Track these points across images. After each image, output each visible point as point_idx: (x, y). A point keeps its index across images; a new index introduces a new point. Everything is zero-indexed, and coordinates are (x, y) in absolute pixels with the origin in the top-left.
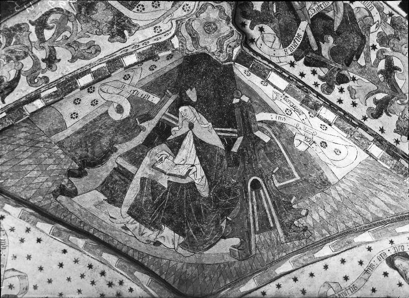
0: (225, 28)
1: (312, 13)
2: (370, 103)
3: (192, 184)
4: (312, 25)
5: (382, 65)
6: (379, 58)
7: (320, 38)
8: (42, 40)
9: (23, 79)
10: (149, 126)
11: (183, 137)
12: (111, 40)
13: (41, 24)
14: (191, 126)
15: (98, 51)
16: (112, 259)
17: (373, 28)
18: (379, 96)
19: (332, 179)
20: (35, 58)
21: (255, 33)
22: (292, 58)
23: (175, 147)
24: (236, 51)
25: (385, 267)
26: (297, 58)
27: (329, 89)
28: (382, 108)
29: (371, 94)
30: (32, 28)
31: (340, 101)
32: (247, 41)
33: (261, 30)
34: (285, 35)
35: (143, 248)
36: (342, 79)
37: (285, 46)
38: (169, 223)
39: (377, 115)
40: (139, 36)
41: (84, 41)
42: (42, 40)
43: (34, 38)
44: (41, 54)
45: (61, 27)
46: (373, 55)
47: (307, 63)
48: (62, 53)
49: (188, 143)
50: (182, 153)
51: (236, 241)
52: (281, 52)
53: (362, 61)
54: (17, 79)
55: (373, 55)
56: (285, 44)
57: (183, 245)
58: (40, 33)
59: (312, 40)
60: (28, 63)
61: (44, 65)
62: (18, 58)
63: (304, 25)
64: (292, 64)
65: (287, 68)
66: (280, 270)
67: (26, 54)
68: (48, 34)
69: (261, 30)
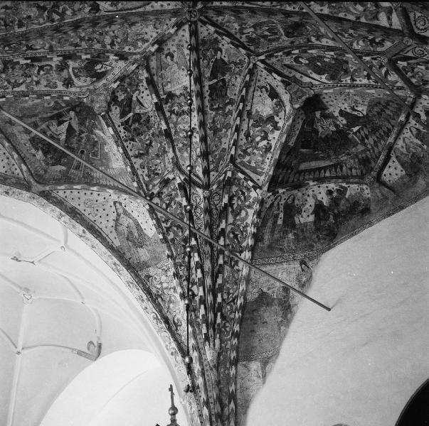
2: (137, 152)
4: (133, 116)
5: (148, 142)
6: (148, 140)
7: (134, 122)
10: (56, 112)
11: (66, 121)
12: (63, 85)
14: (71, 119)
15: (56, 87)
16: (16, 156)
18: (141, 152)
19: (110, 166)
20: (32, 79)
21: (113, 108)
23: (60, 123)
24: (103, 114)
25: (112, 204)
26: (122, 125)
27: (126, 141)
28: (139, 156)
29: (139, 150)
30: (37, 68)
32: (109, 110)
33: (116, 108)
34: (123, 114)
35: (28, 155)
36: (133, 140)
37: (121, 117)
38: (43, 150)
39: (136, 157)
40: (73, 90)
41: (54, 81)
42: (39, 74)
43: (36, 72)
46: (147, 137)
47: (124, 128)
48: (44, 82)
49: (66, 125)
50: (62, 126)
51: (64, 168)
53: (142, 137)
54: (22, 84)
55: (147, 137)
56: (121, 117)
58: (39, 71)
60: (29, 80)
61: (34, 83)
62: (26, 77)
63: (131, 114)
64: (119, 126)
65: (117, 126)
66: (75, 187)
67: (30, 76)
68: (42, 73)
69: (116, 108)
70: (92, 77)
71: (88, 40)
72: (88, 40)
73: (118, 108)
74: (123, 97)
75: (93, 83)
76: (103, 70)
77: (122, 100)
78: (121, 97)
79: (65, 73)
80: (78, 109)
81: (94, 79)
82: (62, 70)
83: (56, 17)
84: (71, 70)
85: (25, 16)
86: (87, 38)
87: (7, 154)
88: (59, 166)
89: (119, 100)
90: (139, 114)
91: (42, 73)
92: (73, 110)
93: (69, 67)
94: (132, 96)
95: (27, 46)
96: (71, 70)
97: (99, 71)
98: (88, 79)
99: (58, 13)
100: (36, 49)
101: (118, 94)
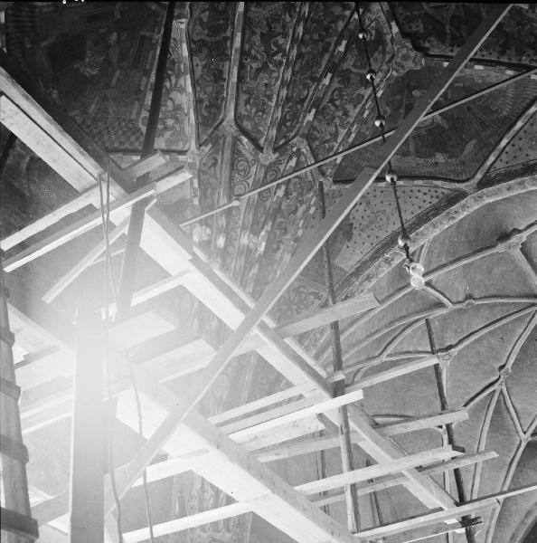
0: (413, 54)
1: (449, 18)
2: (498, 49)
3: (438, 125)
4: (451, 26)
8: (336, 107)
9: (339, 129)
12: (366, 89)
13: (332, 101)
15: (363, 97)
16: (420, 182)
17: (482, 10)
18: (501, 42)
21: (427, 45)
22: (450, 48)
26: (453, 46)
31: (483, 56)
34: (442, 38)
38: (437, 150)
41: (355, 95)
42: (336, 107)
43: (333, 108)
44: (340, 113)
45: (341, 96)
51: (474, 141)
52: (444, 47)
54: (337, 130)
56: (443, 42)
57: (450, 157)
58: (334, 105)
59: (456, 32)
60: (337, 121)
63: (448, 27)
64: (452, 51)
65: (450, 54)
68: (338, 103)
69: (429, 41)
70: (377, 49)
71: (327, 32)
72: (327, 32)
73: (431, 38)
74: (421, 26)
75: (384, 50)
76: (374, 32)
77: (424, 28)
78: (419, 27)
79: (354, 79)
80: (413, 84)
81: (380, 48)
82: (348, 80)
83: (278, 58)
84: (354, 70)
85: (263, 89)
86: (324, 33)
87: (414, 188)
88: (467, 147)
89: (422, 31)
90: (453, 17)
91: (338, 103)
92: (411, 91)
93: (349, 69)
94: (426, 13)
95: (297, 103)
96: (354, 70)
97: (373, 38)
98: (376, 55)
99: (275, 54)
100: (307, 95)
101: (414, 29)
